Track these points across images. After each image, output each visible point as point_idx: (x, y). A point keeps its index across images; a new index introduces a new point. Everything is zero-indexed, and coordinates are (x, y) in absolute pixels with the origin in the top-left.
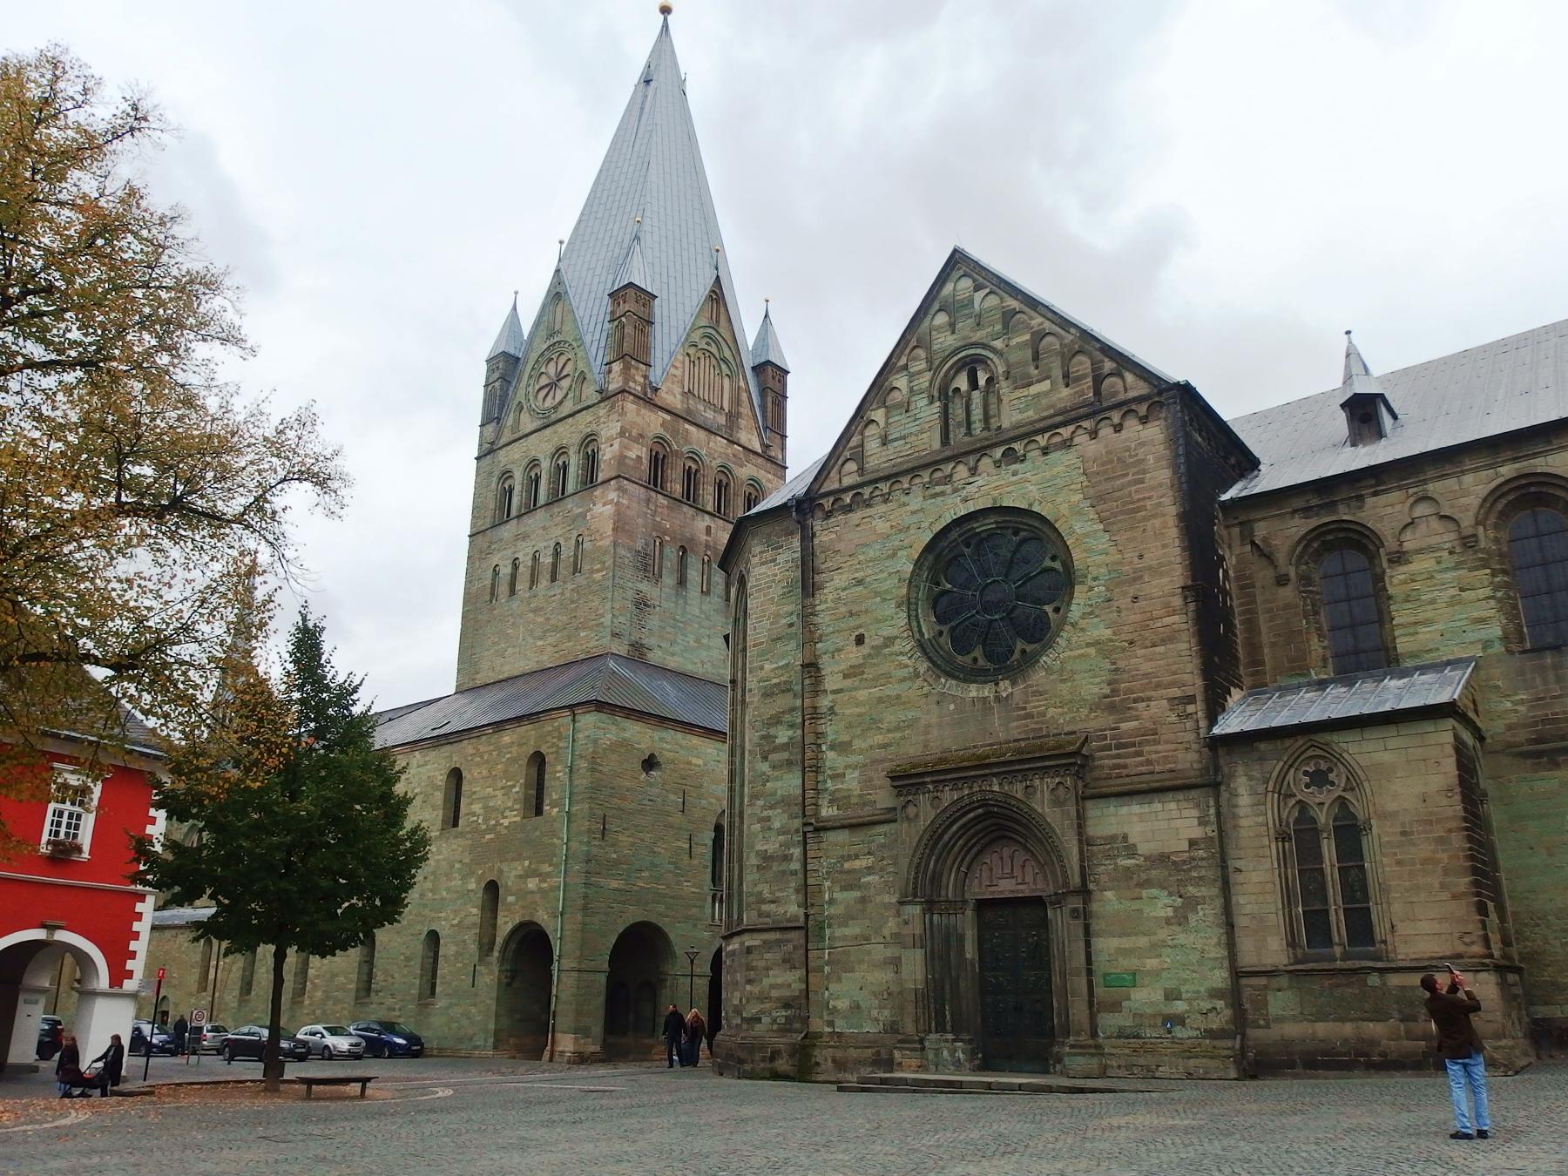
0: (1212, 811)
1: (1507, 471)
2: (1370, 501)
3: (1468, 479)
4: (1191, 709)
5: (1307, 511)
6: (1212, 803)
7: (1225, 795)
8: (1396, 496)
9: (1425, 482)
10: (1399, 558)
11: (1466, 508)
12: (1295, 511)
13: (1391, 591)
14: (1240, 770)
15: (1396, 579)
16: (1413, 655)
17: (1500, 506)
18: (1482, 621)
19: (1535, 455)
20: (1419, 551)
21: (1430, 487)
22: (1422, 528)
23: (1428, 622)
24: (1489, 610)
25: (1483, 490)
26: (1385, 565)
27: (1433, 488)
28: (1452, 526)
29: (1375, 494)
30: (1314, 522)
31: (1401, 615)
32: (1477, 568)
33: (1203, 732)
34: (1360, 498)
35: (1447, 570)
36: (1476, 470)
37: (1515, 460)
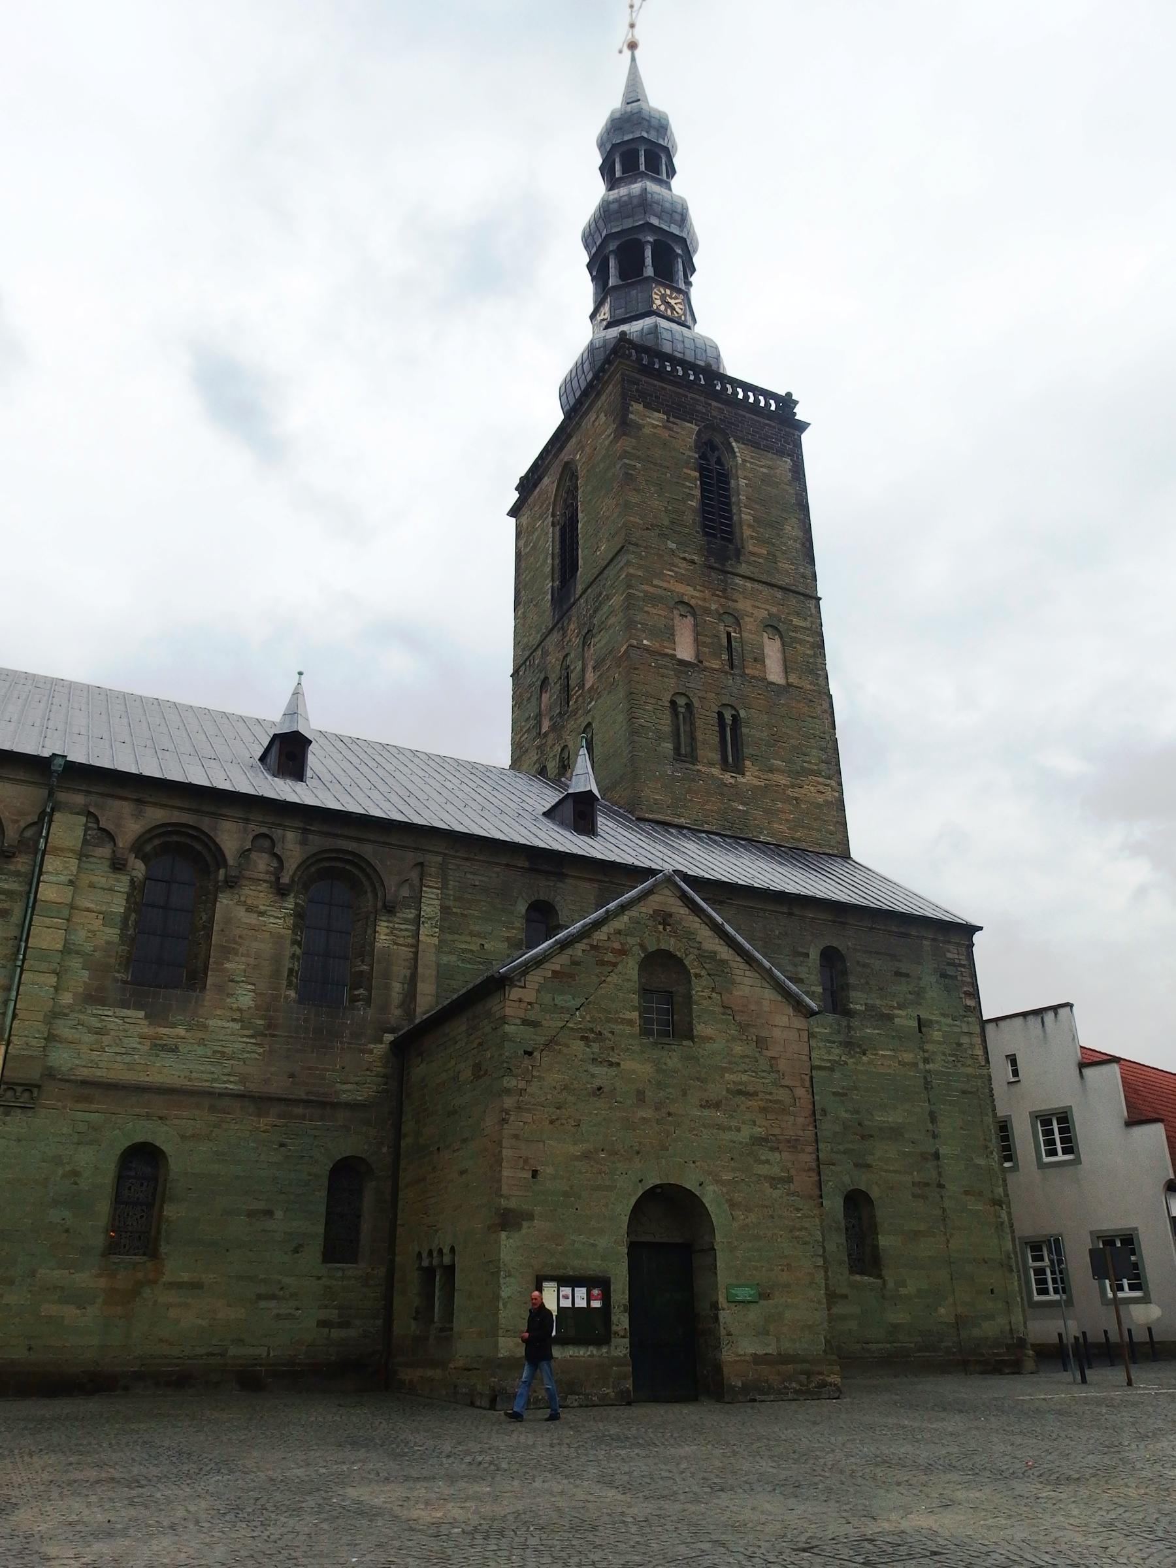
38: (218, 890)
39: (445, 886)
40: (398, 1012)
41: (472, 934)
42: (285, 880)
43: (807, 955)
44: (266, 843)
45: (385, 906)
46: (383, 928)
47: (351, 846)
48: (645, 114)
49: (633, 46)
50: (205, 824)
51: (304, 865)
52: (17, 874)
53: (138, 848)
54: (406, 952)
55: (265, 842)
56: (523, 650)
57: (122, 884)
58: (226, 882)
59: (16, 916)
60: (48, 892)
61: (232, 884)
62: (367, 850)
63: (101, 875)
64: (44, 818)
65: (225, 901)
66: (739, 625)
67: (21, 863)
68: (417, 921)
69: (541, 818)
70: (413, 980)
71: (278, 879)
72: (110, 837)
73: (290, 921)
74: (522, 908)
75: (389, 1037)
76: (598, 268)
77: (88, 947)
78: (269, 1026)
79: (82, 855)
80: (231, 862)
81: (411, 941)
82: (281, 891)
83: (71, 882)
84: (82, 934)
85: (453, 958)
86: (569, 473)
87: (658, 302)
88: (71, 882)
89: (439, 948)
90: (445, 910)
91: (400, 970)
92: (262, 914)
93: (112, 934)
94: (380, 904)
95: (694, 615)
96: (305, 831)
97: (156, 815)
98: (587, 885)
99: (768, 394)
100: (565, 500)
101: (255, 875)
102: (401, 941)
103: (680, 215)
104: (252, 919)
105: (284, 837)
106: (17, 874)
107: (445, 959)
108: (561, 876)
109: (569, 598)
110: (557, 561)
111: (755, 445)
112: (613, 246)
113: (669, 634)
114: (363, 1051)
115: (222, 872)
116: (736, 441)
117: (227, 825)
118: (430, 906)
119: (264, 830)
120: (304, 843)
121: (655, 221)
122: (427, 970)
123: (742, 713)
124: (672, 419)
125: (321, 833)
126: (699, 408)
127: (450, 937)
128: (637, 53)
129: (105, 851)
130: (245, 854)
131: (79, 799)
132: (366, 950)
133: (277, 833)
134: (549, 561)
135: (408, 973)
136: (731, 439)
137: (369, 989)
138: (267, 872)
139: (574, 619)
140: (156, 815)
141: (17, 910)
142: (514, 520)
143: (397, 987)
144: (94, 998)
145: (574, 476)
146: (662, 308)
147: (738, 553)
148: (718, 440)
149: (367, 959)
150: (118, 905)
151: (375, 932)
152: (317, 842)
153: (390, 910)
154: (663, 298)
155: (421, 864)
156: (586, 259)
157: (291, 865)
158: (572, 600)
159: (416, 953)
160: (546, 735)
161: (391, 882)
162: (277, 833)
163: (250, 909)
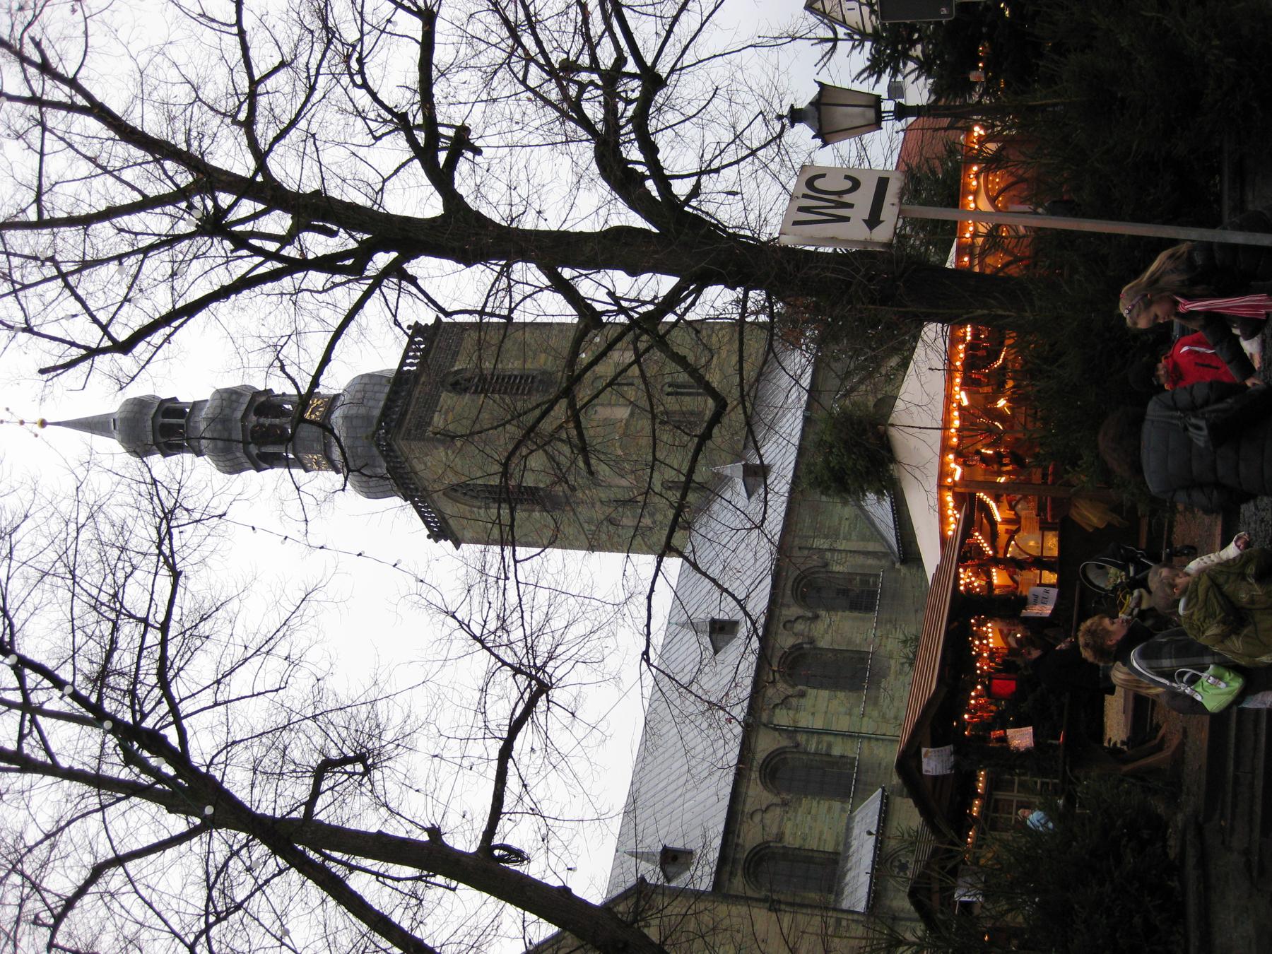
0: (908, 924)
1: (754, 775)
2: (741, 841)
3: (751, 792)
4: (844, 923)
5: (732, 874)
6: (903, 923)
7: (902, 915)
8: (745, 827)
9: (743, 811)
10: (780, 836)
12: (730, 880)
13: (797, 846)
14: (888, 902)
15: (791, 841)
16: (837, 844)
17: (770, 786)
18: (829, 809)
20: (780, 828)
21: (746, 810)
22: (768, 822)
23: (821, 833)
24: (825, 805)
25: (760, 787)
26: (780, 845)
27: (748, 808)
28: (772, 808)
29: (738, 837)
30: (740, 872)
31: (813, 844)
32: (800, 803)
33: (861, 918)
34: (737, 845)
35: (796, 817)
36: (748, 787)
37: (751, 769)
38: (815, 648)
39: (809, 537)
40: (883, 562)
41: (840, 524)
42: (810, 615)
44: (788, 625)
45: (824, 567)
46: (836, 568)
47: (790, 584)
48: (123, 415)
49: (43, 424)
50: (779, 654)
51: (801, 606)
52: (807, 741)
53: (793, 686)
55: (788, 624)
57: (812, 692)
58: (811, 643)
59: (831, 738)
60: (818, 724)
61: (812, 641)
62: (793, 574)
63: (807, 702)
64: (777, 728)
65: (823, 644)
66: (601, 377)
67: (801, 738)
68: (832, 550)
70: (866, 554)
71: (809, 619)
72: (787, 697)
75: (898, 565)
76: (263, 462)
78: (891, 622)
79: (797, 710)
80: (800, 641)
82: (816, 617)
83: (813, 714)
85: (853, 534)
86: (454, 491)
88: (813, 714)
90: (826, 537)
91: (860, 560)
93: (841, 695)
94: (823, 570)
96: (782, 605)
100: (473, 497)
101: (807, 629)
103: (229, 397)
106: (807, 741)
107: (854, 537)
111: (456, 354)
112: (254, 450)
113: (608, 423)
114: (904, 578)
116: (453, 366)
119: (781, 626)
120: (789, 606)
121: (239, 415)
122: (860, 546)
124: (438, 409)
127: (842, 535)
128: (48, 421)
129: (794, 701)
132: (850, 577)
133: (783, 619)
135: (861, 557)
136: (453, 370)
137: (870, 575)
141: (826, 738)
142: (463, 546)
143: (871, 561)
144: (875, 702)
145: (454, 488)
147: (544, 373)
148: (451, 379)
150: (825, 694)
153: (826, 565)
155: (800, 548)
156: (252, 472)
159: (851, 551)
160: (654, 522)
161: (811, 564)
162: (783, 619)
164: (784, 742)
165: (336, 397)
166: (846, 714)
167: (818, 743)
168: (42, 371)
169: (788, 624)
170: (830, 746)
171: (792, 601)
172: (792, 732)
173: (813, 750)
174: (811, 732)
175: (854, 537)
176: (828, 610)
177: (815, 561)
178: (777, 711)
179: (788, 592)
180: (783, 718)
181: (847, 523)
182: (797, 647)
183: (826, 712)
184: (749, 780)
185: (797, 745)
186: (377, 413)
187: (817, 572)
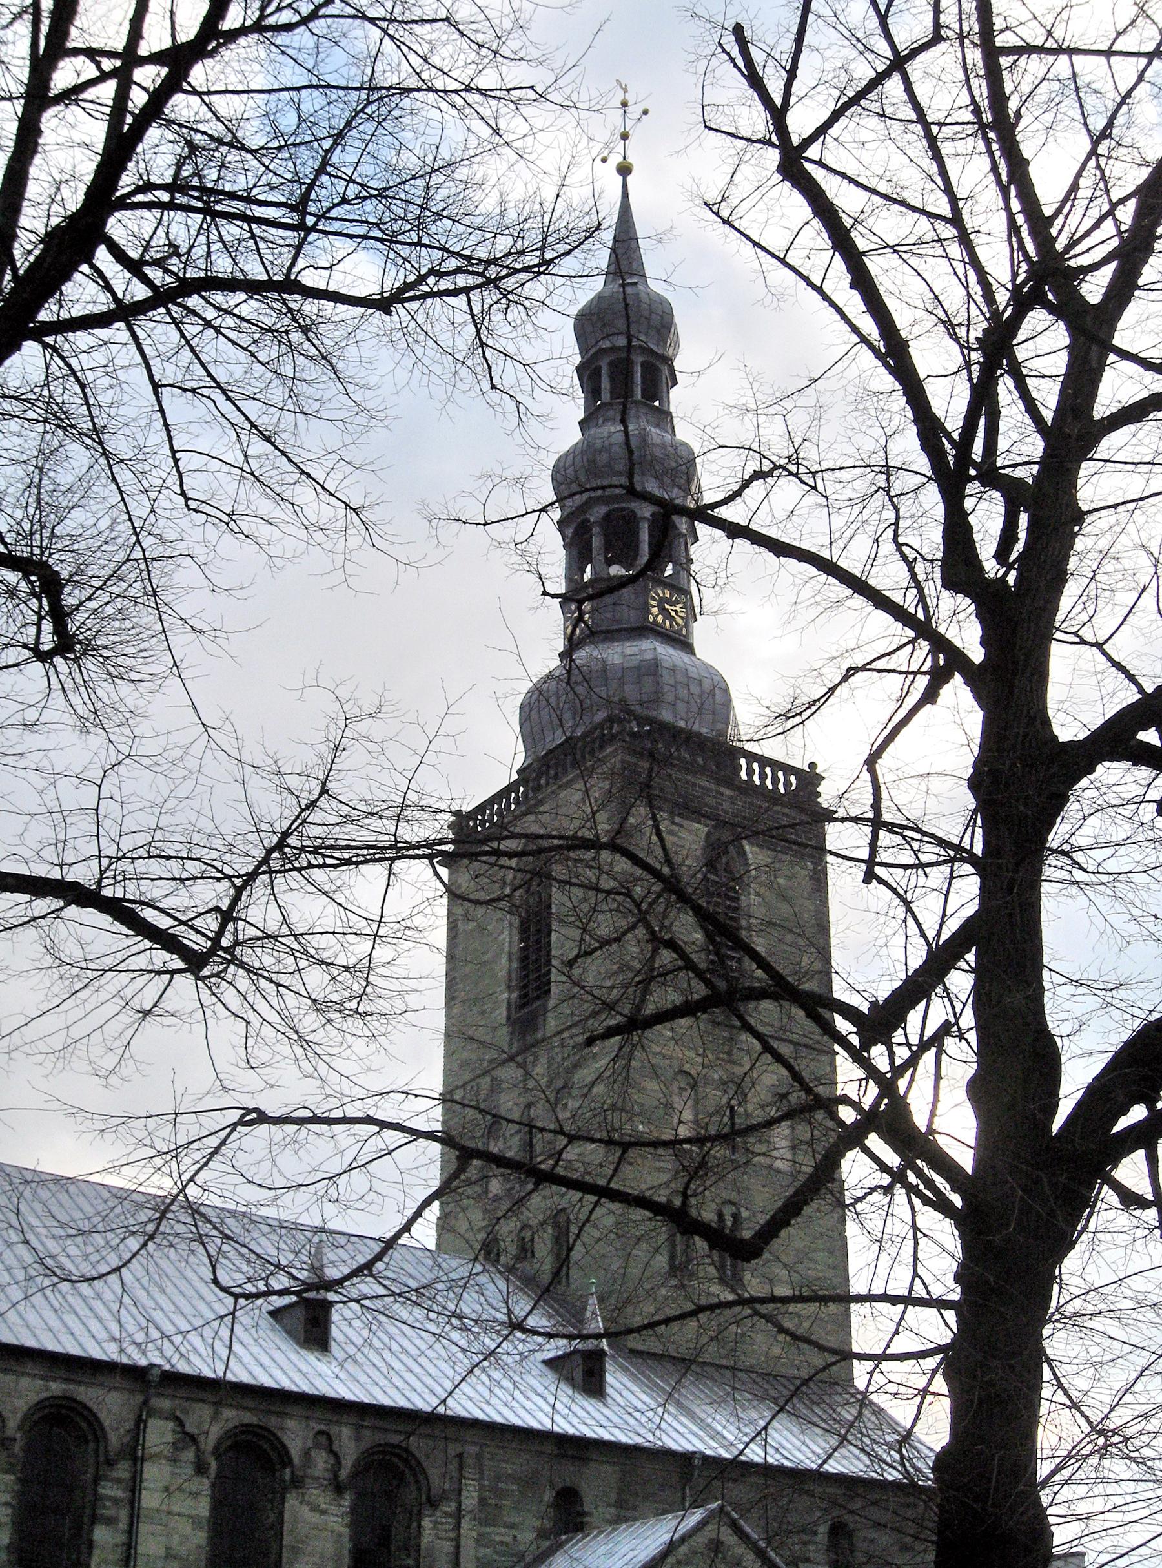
1: (56, 1388)
3: (25, 1382)
11: (14, 1411)
17: (36, 1417)
19: (79, 1383)
25: (34, 1398)
37: (67, 1380)
38: (285, 1490)
41: (505, 1526)
43: (815, 1533)
45: (429, 1500)
49: (624, 170)
50: (273, 1422)
52: (119, 1481)
53: (217, 1452)
54: (448, 1546)
55: (326, 1440)
56: (461, 1066)
57: (204, 1485)
59: (123, 1525)
60: (150, 1499)
61: (297, 1483)
64: (139, 1426)
65: (292, 1502)
67: (123, 1470)
68: (458, 1515)
69: (541, 1366)
71: (336, 1476)
73: (347, 1519)
74: (548, 1496)
77: (183, 1553)
81: (452, 1535)
82: (339, 1489)
83: (166, 1489)
84: (176, 1540)
85: (489, 1551)
87: (655, 610)
89: (480, 1540)
90: (482, 1501)
92: (323, 1512)
93: (200, 1538)
95: (694, 1087)
97: (231, 1416)
98: (609, 1468)
99: (788, 769)
102: (443, 1534)
104: (315, 1518)
105: (340, 1435)
106: (119, 1481)
107: (482, 1552)
108: (585, 1460)
109: (535, 1030)
110: (515, 965)
112: (598, 512)
115: (288, 1471)
117: (290, 1423)
118: (470, 1500)
119: (323, 1427)
120: (358, 1439)
123: (745, 1214)
125: (374, 1428)
126: (707, 799)
128: (629, 178)
129: (189, 1455)
130: (307, 1453)
131: (165, 1404)
134: (504, 961)
138: (326, 1470)
139: (543, 1060)
140: (231, 1416)
141: (124, 1514)
146: (660, 618)
149: (413, 1554)
150: (203, 1508)
151: (420, 1526)
152: (370, 1438)
153: (433, 1504)
154: (662, 602)
157: (348, 1462)
158: (540, 1035)
159: (458, 1547)
161: (435, 1475)
162: (334, 1430)
163: (315, 1508)
164: (115, 1440)
165: (687, 646)
166: (168, 1549)
167: (116, 1501)
168: (738, 30)
169: (326, 1440)
170: (111, 1521)
171: (365, 1445)
172: (135, 1454)
173: (102, 1491)
174: (134, 1487)
175: (482, 1552)
176: (353, 1510)
177: (437, 1480)
178: (171, 1425)
179: (382, 1438)
180: (159, 1433)
181: (508, 1539)
182: (284, 1456)
183: (169, 1513)
184: (45, 1378)
185: (110, 1463)
186: (666, 716)
187: (419, 1489)
